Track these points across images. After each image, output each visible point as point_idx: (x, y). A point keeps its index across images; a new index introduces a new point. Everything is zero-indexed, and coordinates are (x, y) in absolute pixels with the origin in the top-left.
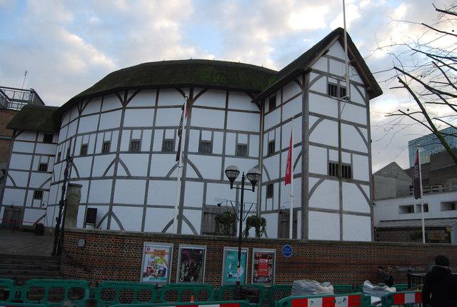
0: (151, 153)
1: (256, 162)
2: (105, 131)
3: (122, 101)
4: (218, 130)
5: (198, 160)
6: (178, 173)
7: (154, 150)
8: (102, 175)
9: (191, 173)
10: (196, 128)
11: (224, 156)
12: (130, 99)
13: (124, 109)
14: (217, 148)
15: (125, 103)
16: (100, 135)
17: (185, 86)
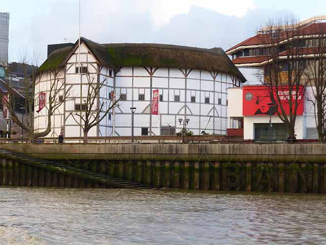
0: (168, 101)
1: (213, 106)
2: (139, 88)
3: (149, 72)
4: (197, 90)
5: (190, 105)
6: (183, 112)
7: (170, 100)
8: (141, 112)
9: (188, 112)
10: (189, 90)
11: (200, 103)
12: (155, 71)
13: (151, 77)
14: (197, 100)
15: (151, 74)
16: (136, 91)
17: (183, 68)
